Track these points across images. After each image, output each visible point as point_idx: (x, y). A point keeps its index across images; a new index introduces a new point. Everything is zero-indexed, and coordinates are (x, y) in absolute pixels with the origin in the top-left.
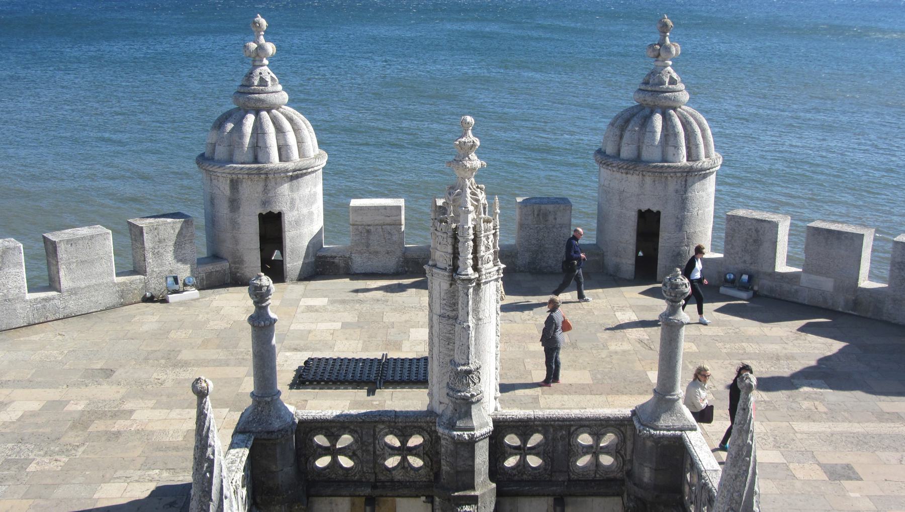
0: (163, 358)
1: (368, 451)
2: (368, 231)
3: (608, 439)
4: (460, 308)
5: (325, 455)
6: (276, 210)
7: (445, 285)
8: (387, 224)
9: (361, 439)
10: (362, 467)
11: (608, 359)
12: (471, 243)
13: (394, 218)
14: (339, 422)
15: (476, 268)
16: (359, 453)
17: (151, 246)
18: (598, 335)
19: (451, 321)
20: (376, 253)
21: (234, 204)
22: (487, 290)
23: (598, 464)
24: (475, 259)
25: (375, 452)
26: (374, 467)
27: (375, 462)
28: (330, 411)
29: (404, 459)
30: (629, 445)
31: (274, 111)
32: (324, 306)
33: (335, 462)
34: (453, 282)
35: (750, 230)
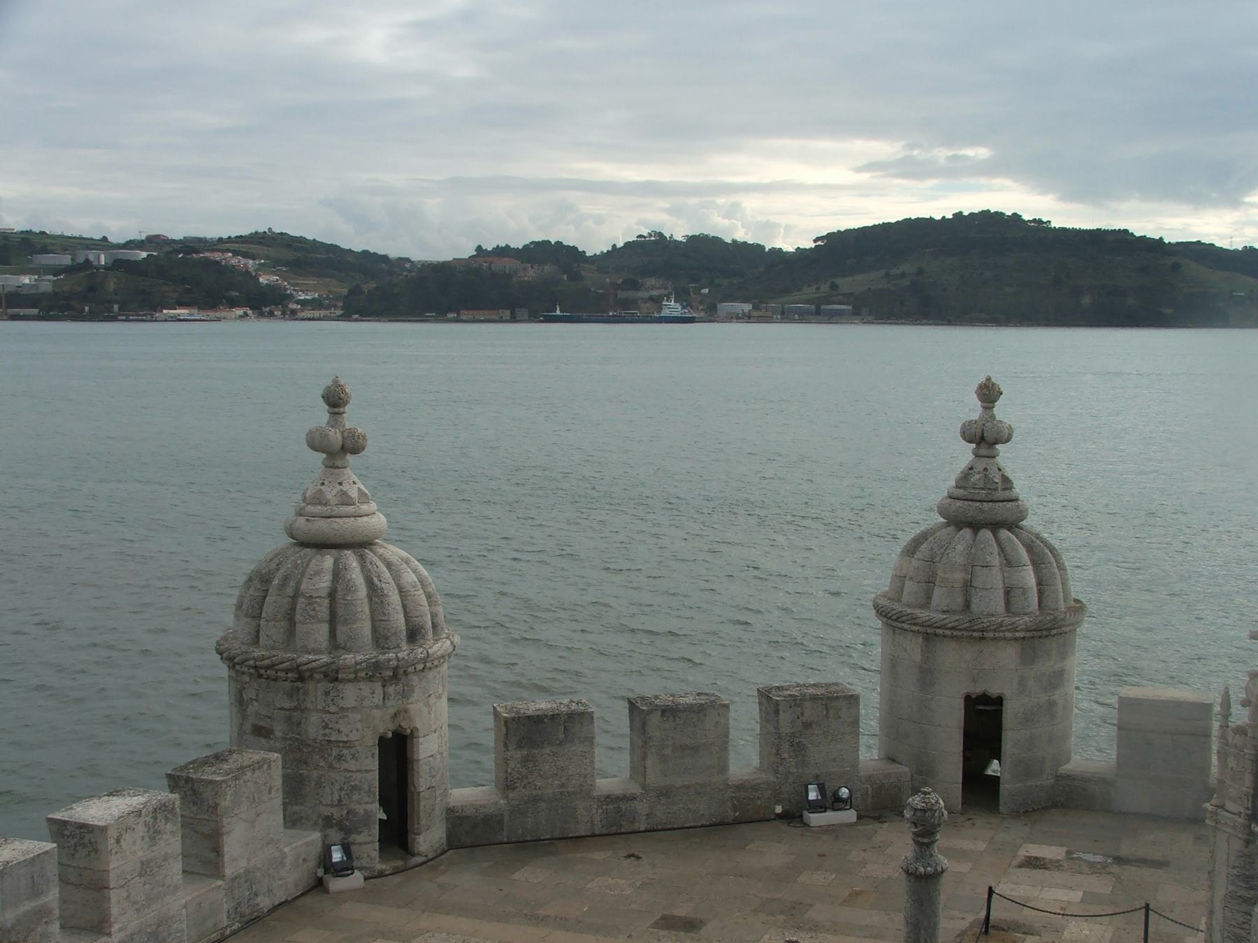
0: (782, 912)
6: (994, 691)
7: (1237, 845)
19: (1244, 907)
21: (927, 675)
31: (1004, 534)
32: (1058, 861)
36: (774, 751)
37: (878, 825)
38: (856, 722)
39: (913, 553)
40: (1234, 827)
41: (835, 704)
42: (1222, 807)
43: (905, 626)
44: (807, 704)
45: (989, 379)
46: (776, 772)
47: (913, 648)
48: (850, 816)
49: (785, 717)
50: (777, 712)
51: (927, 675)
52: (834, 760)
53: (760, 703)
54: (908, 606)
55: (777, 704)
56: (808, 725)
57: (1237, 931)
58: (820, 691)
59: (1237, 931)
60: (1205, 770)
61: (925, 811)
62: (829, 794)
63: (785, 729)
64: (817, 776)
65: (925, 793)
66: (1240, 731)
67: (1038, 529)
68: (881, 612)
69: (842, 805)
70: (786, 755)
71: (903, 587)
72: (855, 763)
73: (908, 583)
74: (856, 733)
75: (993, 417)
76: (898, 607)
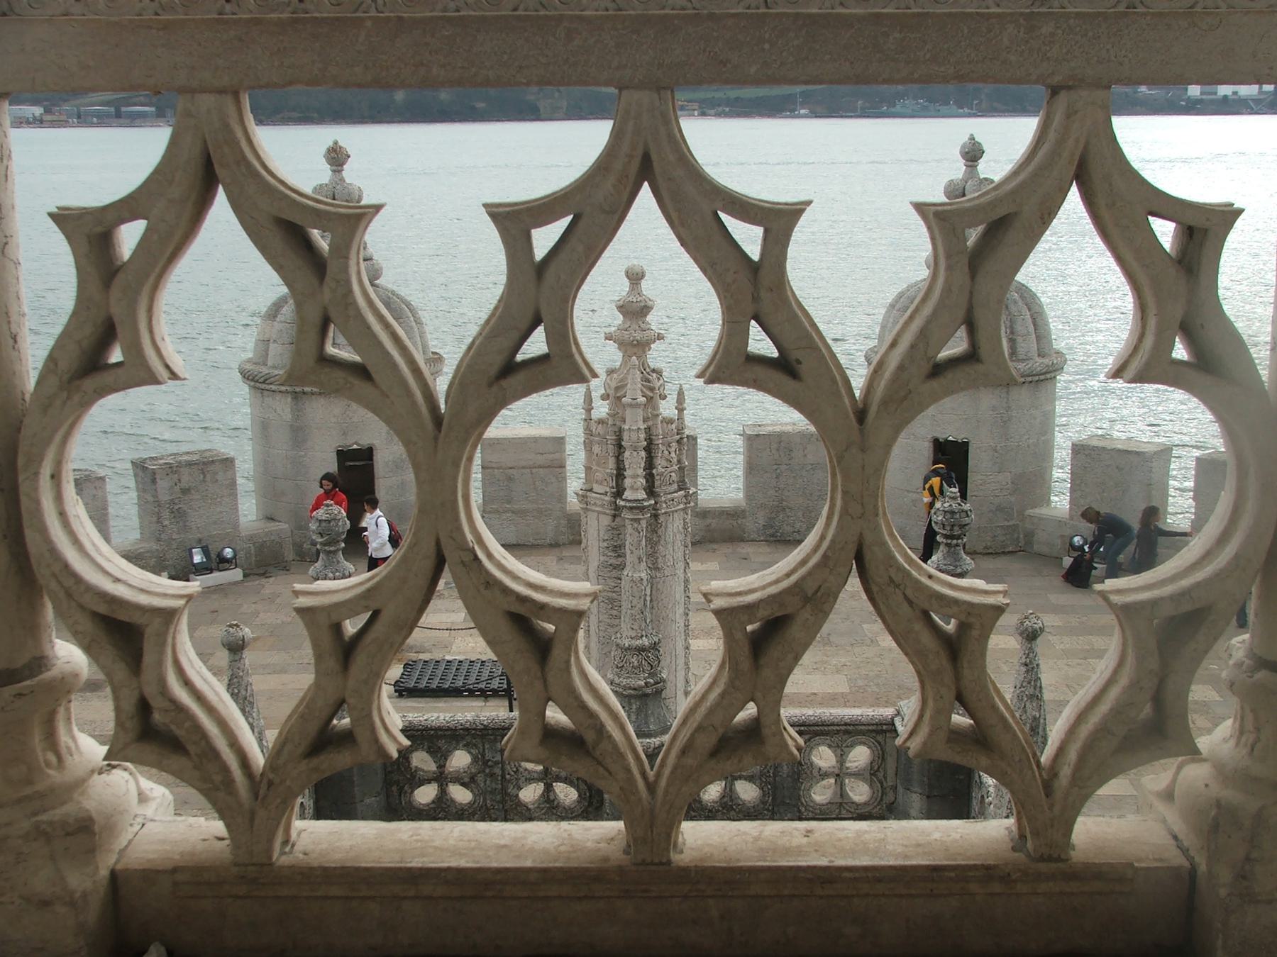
1: (492, 775)
2: (510, 479)
3: (860, 755)
4: (628, 552)
5: (429, 781)
6: (365, 442)
7: (606, 520)
8: (540, 467)
9: (483, 756)
10: (485, 800)
11: (877, 660)
12: (643, 454)
13: (551, 456)
14: (449, 729)
15: (651, 491)
16: (480, 778)
17: (167, 498)
18: (865, 626)
19: (615, 573)
20: (522, 513)
21: (298, 433)
22: (670, 525)
23: (842, 793)
24: (650, 478)
25: (503, 777)
26: (503, 801)
27: (504, 791)
28: (436, 715)
29: (549, 788)
30: (891, 765)
33: (443, 792)
34: (616, 512)
35: (1108, 466)
36: (155, 519)
37: (264, 581)
38: (233, 484)
39: (275, 316)
40: (603, 506)
41: (210, 470)
42: (591, 490)
43: (273, 387)
44: (185, 471)
45: (336, 143)
46: (159, 540)
47: (282, 407)
48: (236, 574)
49: (163, 484)
50: (154, 481)
51: (298, 433)
52: (215, 523)
53: (136, 475)
54: (274, 367)
55: (154, 472)
56: (186, 491)
57: (610, 594)
58: (195, 458)
59: (610, 594)
60: (562, 497)
61: (329, 522)
62: (213, 556)
63: (164, 497)
64: (200, 541)
65: (328, 505)
66: (601, 422)
67: (390, 286)
68: (247, 376)
69: (227, 565)
70: (167, 523)
71: (267, 351)
72: (236, 525)
73: (272, 346)
74: (234, 495)
75: (342, 180)
76: (265, 370)
